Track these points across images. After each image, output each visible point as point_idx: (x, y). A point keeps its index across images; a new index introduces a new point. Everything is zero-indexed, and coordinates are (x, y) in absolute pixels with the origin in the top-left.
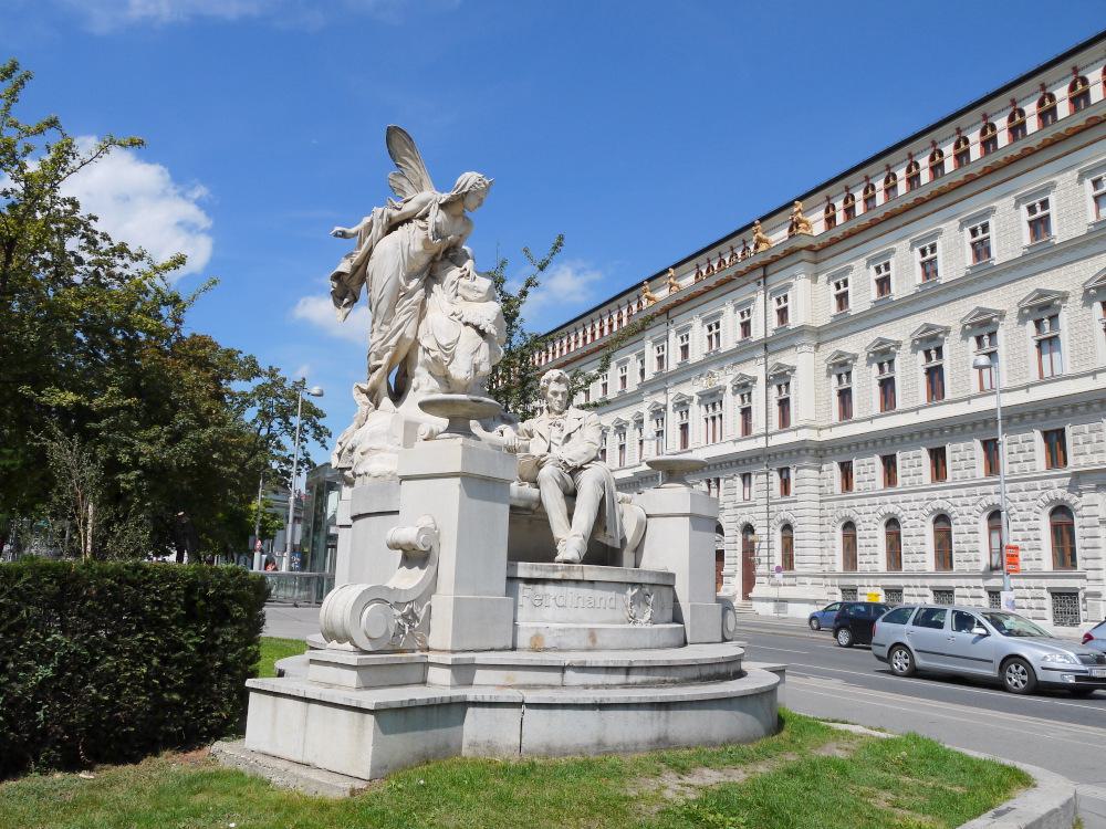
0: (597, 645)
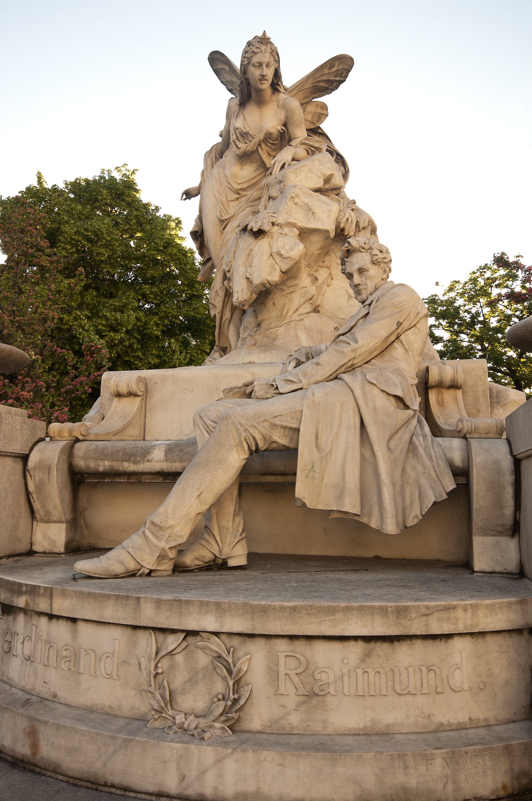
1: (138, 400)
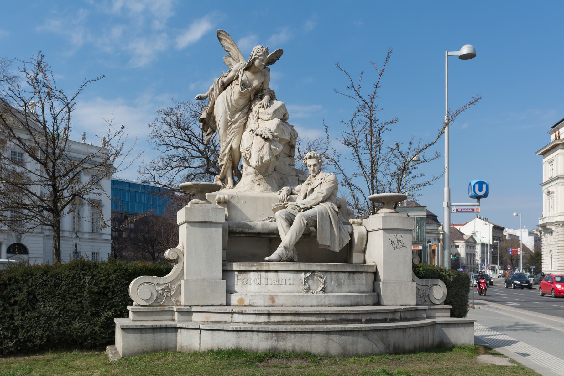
0: (275, 304)
1: (226, 205)
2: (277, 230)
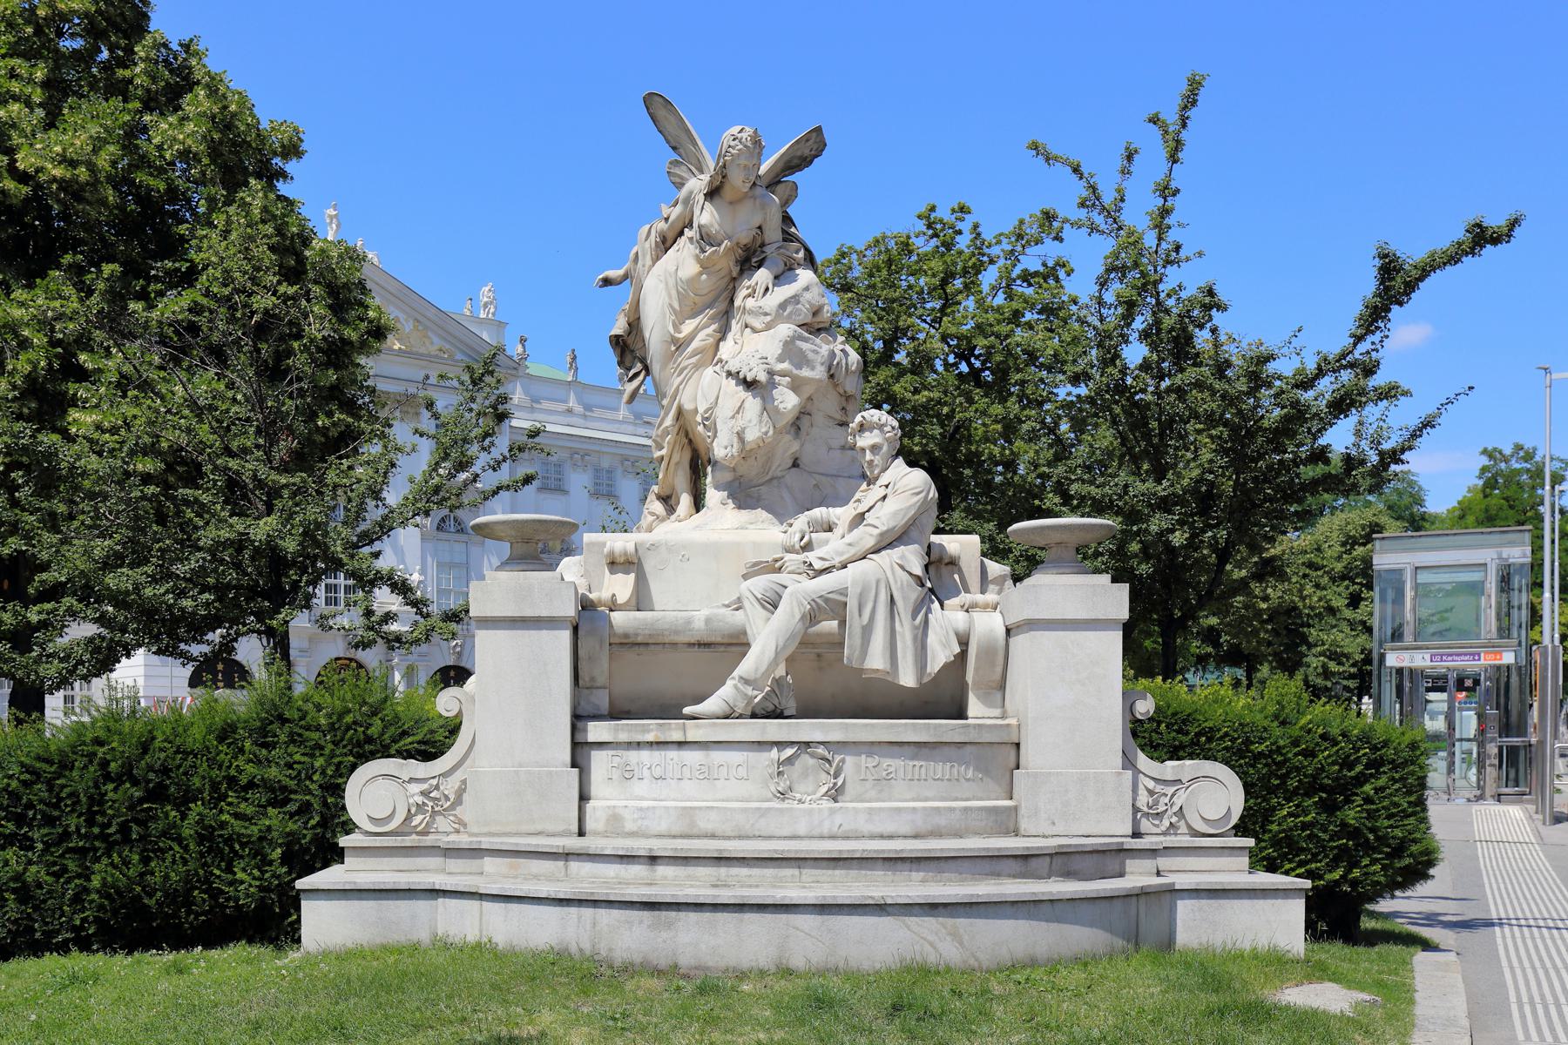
2: (745, 633)
